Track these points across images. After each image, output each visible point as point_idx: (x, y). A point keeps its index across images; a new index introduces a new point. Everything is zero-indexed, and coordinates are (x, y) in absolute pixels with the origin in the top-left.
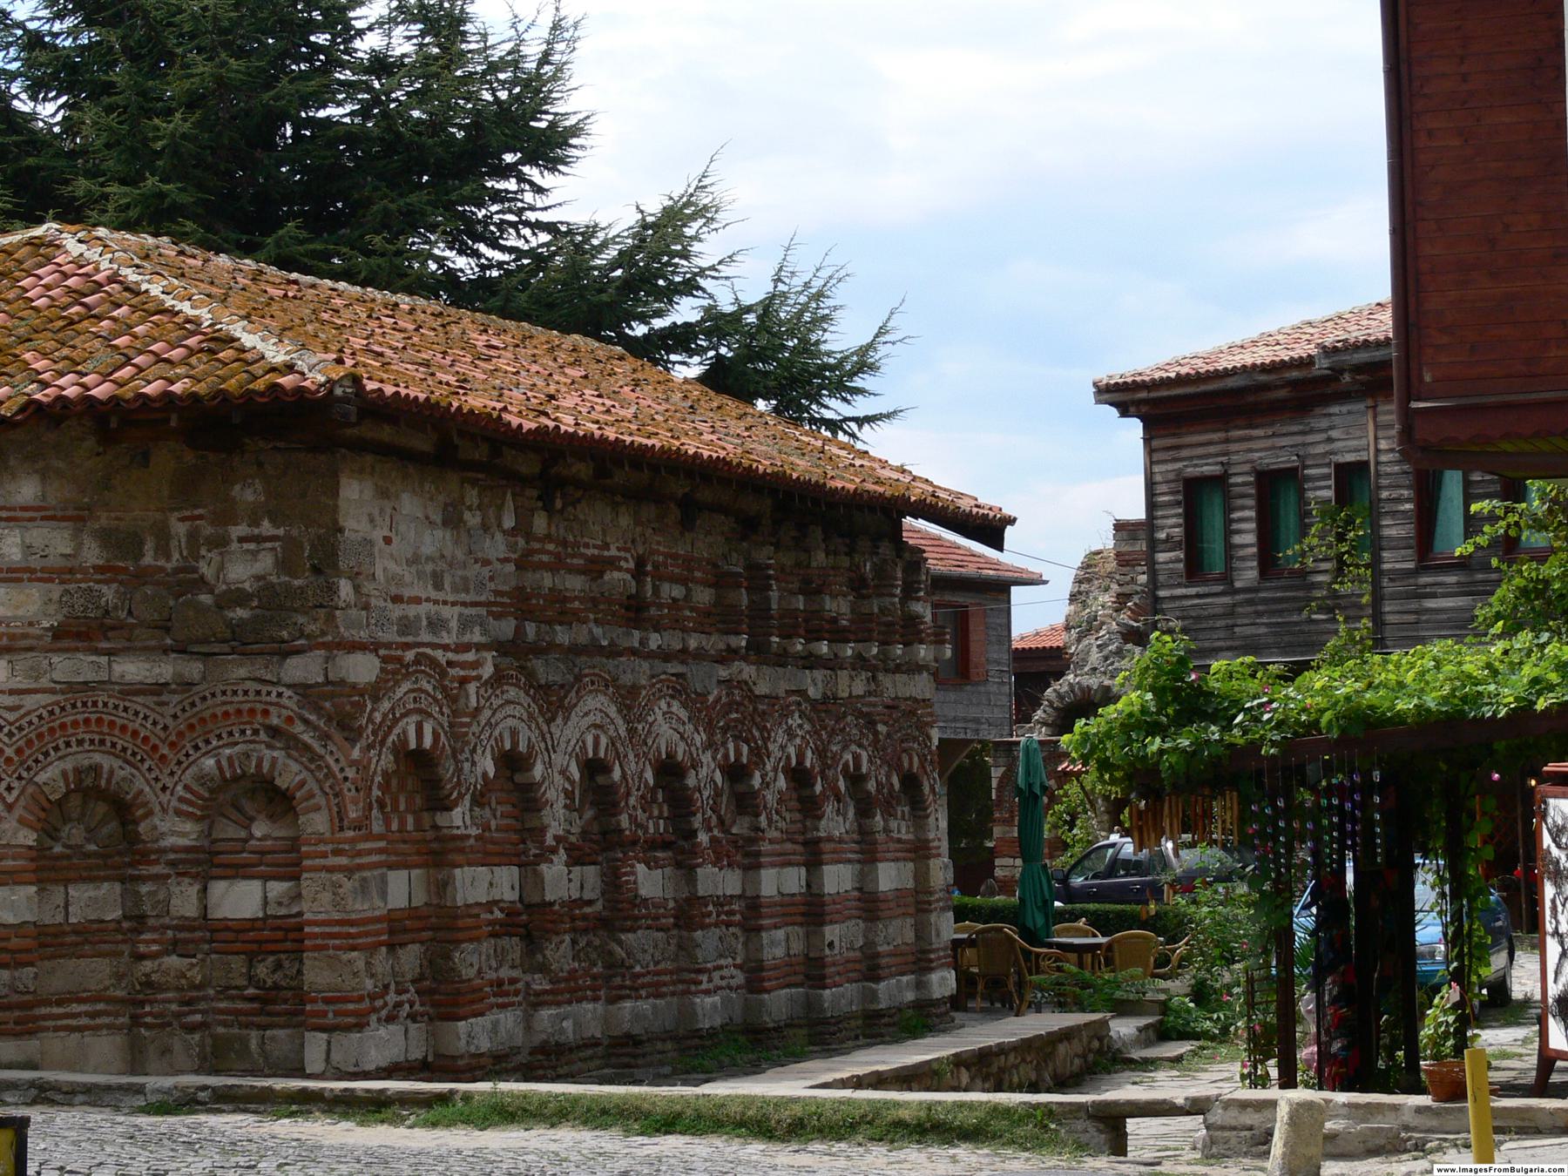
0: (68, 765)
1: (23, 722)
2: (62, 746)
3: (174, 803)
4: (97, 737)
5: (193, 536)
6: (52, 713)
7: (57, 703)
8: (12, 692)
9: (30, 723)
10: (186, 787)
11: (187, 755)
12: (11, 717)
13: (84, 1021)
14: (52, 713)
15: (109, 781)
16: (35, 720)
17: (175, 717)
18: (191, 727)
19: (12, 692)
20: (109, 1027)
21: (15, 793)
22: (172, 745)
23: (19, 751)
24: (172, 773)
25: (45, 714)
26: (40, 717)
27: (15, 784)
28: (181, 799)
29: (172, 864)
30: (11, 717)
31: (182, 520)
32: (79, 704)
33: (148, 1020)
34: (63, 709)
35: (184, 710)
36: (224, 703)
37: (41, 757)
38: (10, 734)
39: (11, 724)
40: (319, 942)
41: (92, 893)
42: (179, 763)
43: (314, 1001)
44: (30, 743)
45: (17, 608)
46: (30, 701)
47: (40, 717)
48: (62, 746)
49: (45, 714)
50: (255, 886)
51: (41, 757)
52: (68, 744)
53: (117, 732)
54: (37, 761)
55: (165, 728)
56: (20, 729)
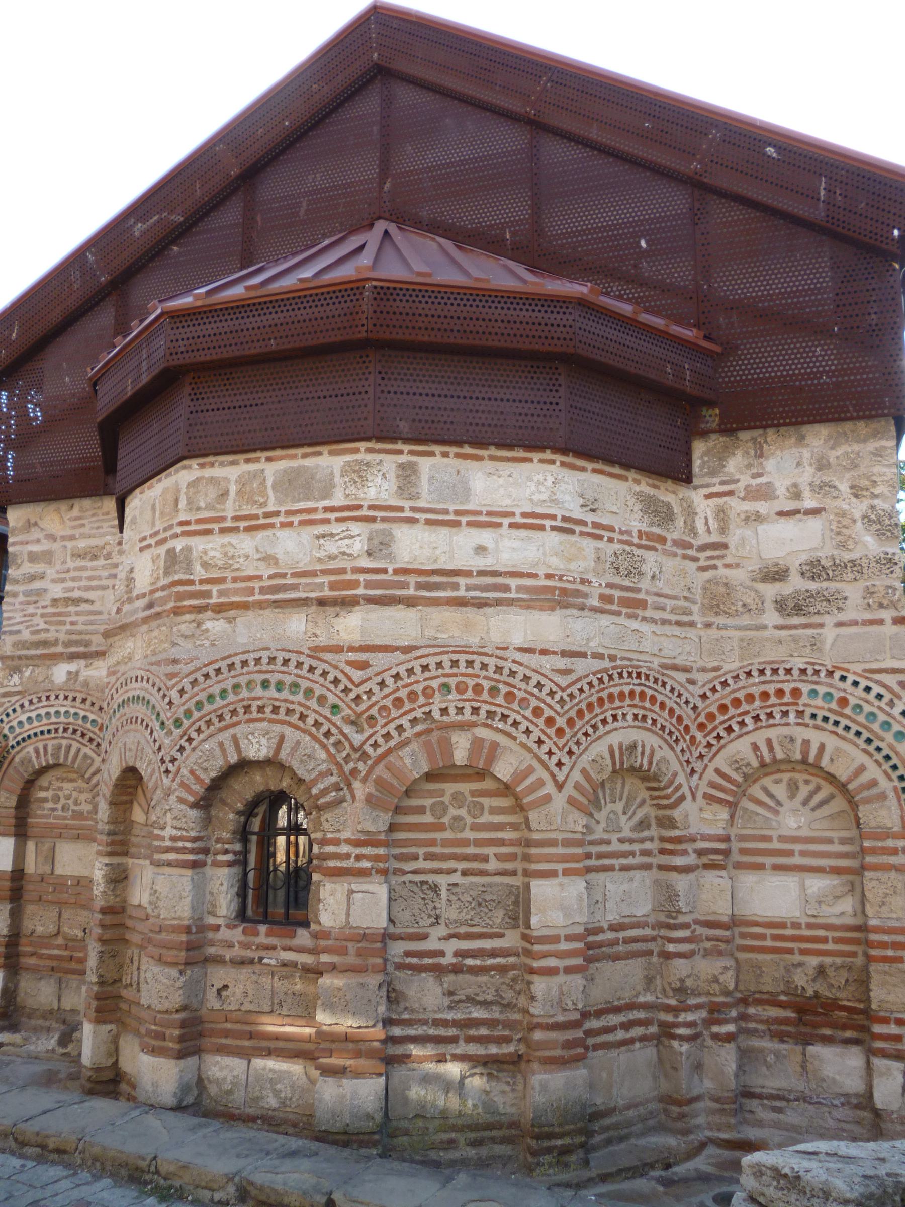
0: (615, 739)
1: (574, 689)
2: (610, 719)
3: (704, 788)
4: (641, 712)
5: (722, 514)
6: (601, 680)
7: (605, 670)
8: (564, 654)
9: (581, 690)
10: (718, 771)
11: (719, 737)
12: (563, 681)
13: (620, 1035)
14: (601, 680)
15: (650, 763)
16: (586, 688)
17: (704, 696)
18: (723, 708)
19: (564, 654)
20: (642, 1039)
21: (565, 769)
22: (701, 726)
23: (570, 722)
24: (701, 757)
25: (595, 682)
26: (590, 684)
27: (565, 760)
28: (712, 785)
29: (700, 853)
30: (563, 681)
31: (708, 497)
32: (625, 675)
33: (681, 1031)
34: (611, 677)
35: (714, 690)
36: (764, 683)
37: (590, 731)
38: (562, 701)
39: (563, 690)
40: (890, 953)
41: (626, 886)
42: (709, 745)
43: (885, 1021)
44: (580, 713)
45: (570, 560)
46: (581, 666)
47: (590, 684)
48: (610, 719)
49: (595, 682)
50: (791, 881)
51: (590, 731)
52: (615, 717)
53: (656, 708)
54: (586, 734)
55: (695, 708)
56: (571, 696)
